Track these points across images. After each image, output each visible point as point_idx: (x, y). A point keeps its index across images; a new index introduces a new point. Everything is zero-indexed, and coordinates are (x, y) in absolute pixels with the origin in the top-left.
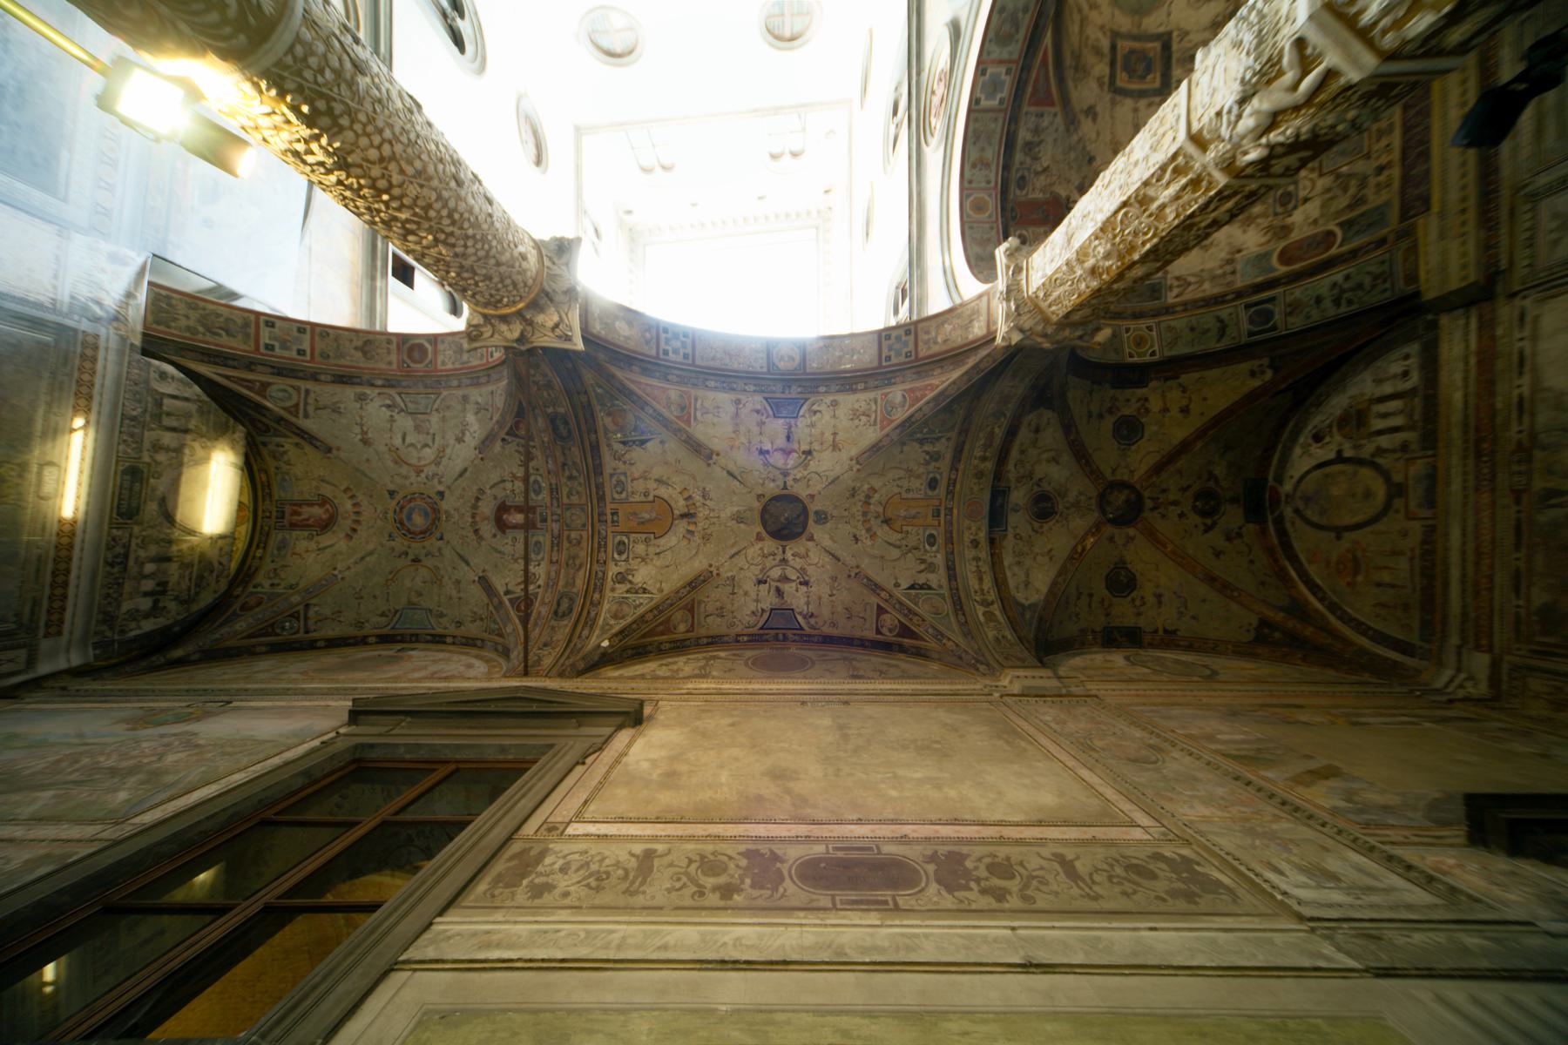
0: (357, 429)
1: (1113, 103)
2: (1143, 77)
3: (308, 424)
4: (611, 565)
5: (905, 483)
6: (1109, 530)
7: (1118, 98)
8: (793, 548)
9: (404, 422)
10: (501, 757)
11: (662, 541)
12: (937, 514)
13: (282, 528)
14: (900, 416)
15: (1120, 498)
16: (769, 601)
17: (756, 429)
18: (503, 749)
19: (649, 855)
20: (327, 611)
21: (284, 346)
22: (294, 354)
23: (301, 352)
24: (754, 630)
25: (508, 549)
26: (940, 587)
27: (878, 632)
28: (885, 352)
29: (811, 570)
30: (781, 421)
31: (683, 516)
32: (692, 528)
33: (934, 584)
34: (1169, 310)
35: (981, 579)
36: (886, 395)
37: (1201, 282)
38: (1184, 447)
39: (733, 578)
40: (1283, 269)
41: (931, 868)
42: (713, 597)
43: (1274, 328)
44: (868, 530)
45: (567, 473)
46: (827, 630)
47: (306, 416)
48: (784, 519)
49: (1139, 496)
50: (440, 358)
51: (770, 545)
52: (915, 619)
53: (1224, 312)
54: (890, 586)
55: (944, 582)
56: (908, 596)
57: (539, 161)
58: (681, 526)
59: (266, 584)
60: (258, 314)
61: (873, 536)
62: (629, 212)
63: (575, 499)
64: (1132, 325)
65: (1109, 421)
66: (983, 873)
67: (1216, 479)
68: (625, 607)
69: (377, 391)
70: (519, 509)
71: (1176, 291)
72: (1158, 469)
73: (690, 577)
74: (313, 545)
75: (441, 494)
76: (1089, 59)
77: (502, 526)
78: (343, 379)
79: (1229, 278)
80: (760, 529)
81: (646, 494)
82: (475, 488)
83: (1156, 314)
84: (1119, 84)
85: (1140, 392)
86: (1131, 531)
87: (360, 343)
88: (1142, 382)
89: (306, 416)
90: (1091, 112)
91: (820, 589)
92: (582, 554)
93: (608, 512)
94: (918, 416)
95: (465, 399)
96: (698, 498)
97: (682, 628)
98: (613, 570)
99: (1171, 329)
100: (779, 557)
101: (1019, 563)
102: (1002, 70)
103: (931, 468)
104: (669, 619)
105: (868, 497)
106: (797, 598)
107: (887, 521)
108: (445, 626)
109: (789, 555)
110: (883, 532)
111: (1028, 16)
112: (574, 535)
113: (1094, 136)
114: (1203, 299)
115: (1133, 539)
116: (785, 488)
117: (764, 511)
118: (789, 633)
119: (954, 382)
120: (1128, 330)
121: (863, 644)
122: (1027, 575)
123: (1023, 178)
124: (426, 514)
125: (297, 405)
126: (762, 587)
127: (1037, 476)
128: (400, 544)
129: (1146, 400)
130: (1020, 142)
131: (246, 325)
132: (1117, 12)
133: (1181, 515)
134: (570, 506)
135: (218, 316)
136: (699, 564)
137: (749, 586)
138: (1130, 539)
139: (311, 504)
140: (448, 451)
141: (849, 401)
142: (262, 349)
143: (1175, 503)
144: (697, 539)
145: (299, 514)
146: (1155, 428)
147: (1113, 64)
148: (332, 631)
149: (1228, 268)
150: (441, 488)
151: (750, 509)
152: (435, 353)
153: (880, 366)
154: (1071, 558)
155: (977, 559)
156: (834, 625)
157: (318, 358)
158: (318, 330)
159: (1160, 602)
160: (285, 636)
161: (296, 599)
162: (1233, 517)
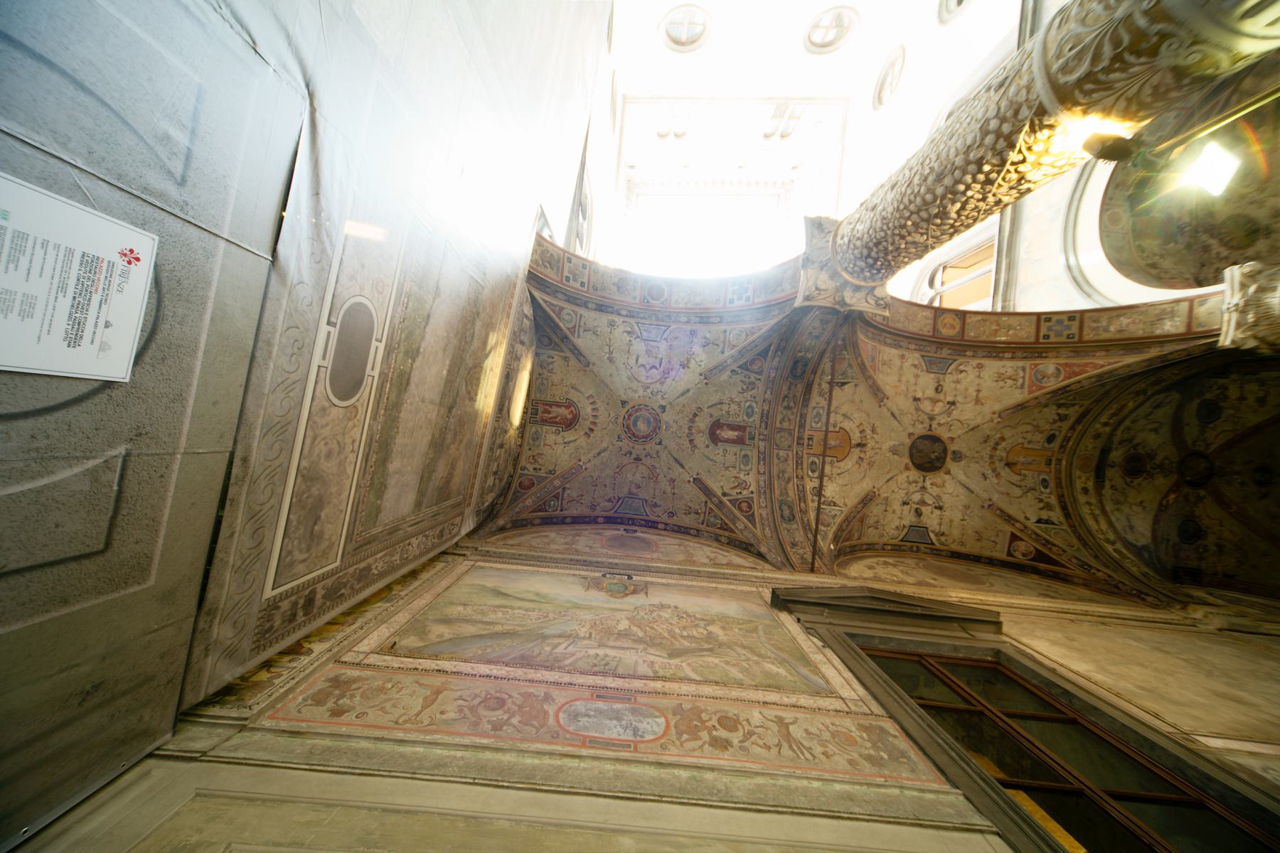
0: (606, 349)
3: (579, 342)
4: (807, 480)
5: (1029, 436)
8: (931, 478)
10: (954, 655)
11: (842, 464)
12: (1049, 463)
13: (536, 422)
14: (1052, 384)
16: (909, 519)
17: (912, 380)
18: (956, 648)
20: (574, 494)
22: (578, 285)
23: (582, 284)
25: (719, 458)
27: (1009, 554)
28: (1043, 331)
29: (945, 498)
30: (932, 375)
31: (859, 445)
33: (1055, 520)
35: (1097, 521)
36: (1036, 365)
39: (886, 499)
44: (994, 470)
45: (785, 404)
46: (955, 547)
51: (914, 474)
52: (1055, 549)
54: (1022, 518)
58: (856, 452)
59: (531, 468)
61: (998, 476)
62: (632, 167)
63: (786, 425)
70: (732, 427)
72: (1229, 445)
73: (863, 494)
74: (559, 439)
75: (663, 408)
77: (714, 439)
78: (601, 308)
80: (907, 460)
82: (694, 406)
85: (1221, 381)
86: (1202, 493)
92: (789, 469)
93: (806, 437)
94: (1073, 387)
95: (693, 333)
100: (920, 485)
101: (1118, 510)
103: (1055, 426)
105: (997, 444)
106: (931, 519)
107: (1008, 465)
108: (659, 515)
109: (928, 484)
110: (1005, 472)
112: (782, 453)
115: (1204, 497)
116: (930, 430)
117: (912, 447)
118: (922, 546)
119: (1129, 366)
121: (991, 562)
122: (1128, 520)
124: (649, 422)
126: (907, 507)
127: (1135, 442)
128: (626, 444)
134: (781, 430)
136: (866, 486)
137: (896, 506)
138: (1200, 499)
140: (673, 373)
141: (993, 367)
142: (1041, 340)
144: (865, 464)
145: (549, 413)
146: (1232, 412)
148: (575, 511)
150: (663, 403)
153: (1037, 342)
155: (1089, 504)
157: (591, 290)
160: (550, 513)
161: (557, 483)
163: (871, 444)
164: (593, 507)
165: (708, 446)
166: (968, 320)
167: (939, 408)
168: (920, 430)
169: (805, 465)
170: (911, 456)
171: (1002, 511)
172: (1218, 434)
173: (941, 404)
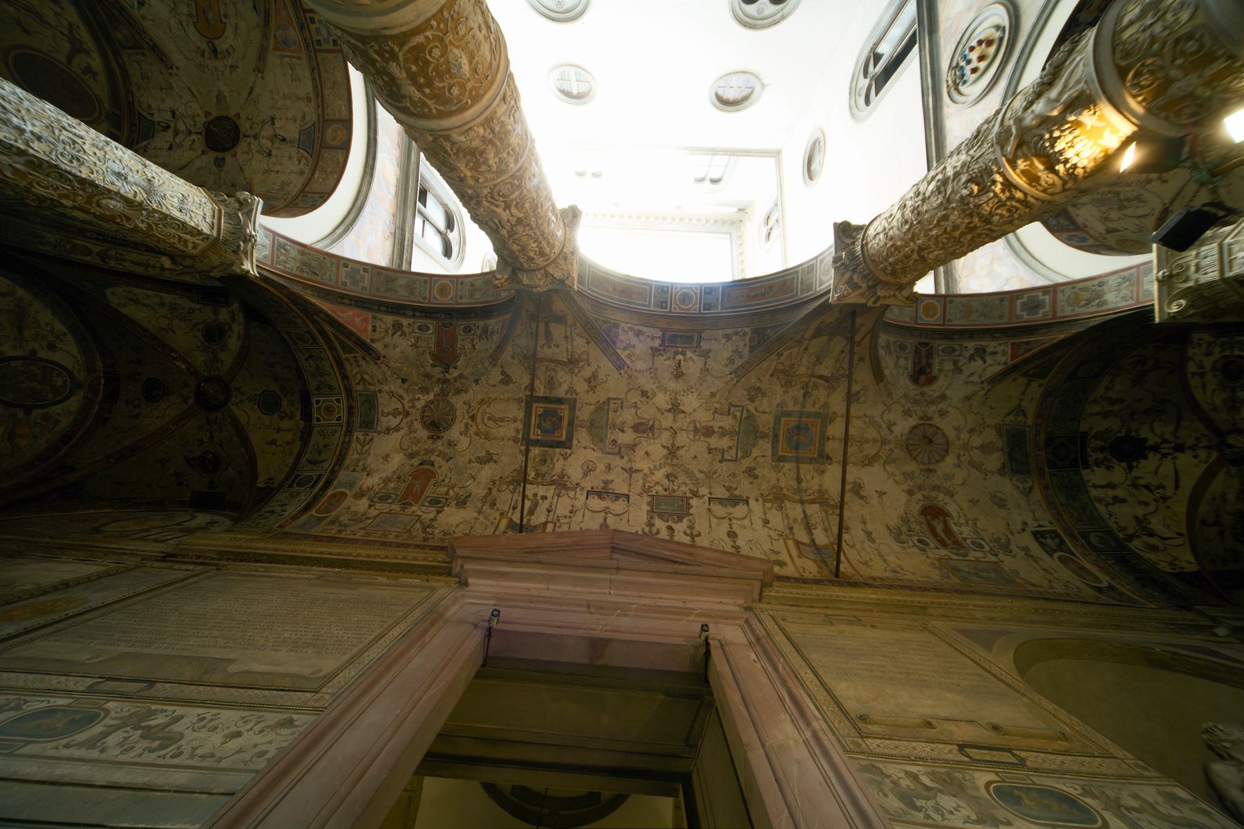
1: (519, 401)
2: (539, 427)
8: (199, 140)
11: (192, 28)
30: (297, 136)
34: (349, 432)
35: (138, 264)
38: (245, 440)
39: (172, 88)
71: (361, 437)
80: (215, 113)
84: (535, 405)
86: (191, 401)
90: (507, 380)
96: (229, 62)
99: (334, 433)
100: (192, 129)
113: (492, 382)
116: (245, 136)
117: (227, 118)
120: (338, 401)
132: (593, 407)
133: (201, 441)
136: (177, 58)
143: (212, 437)
147: (546, 399)
166: (339, 152)
167: (266, 143)
168: (244, 126)
170: (219, 118)
173: (269, 145)
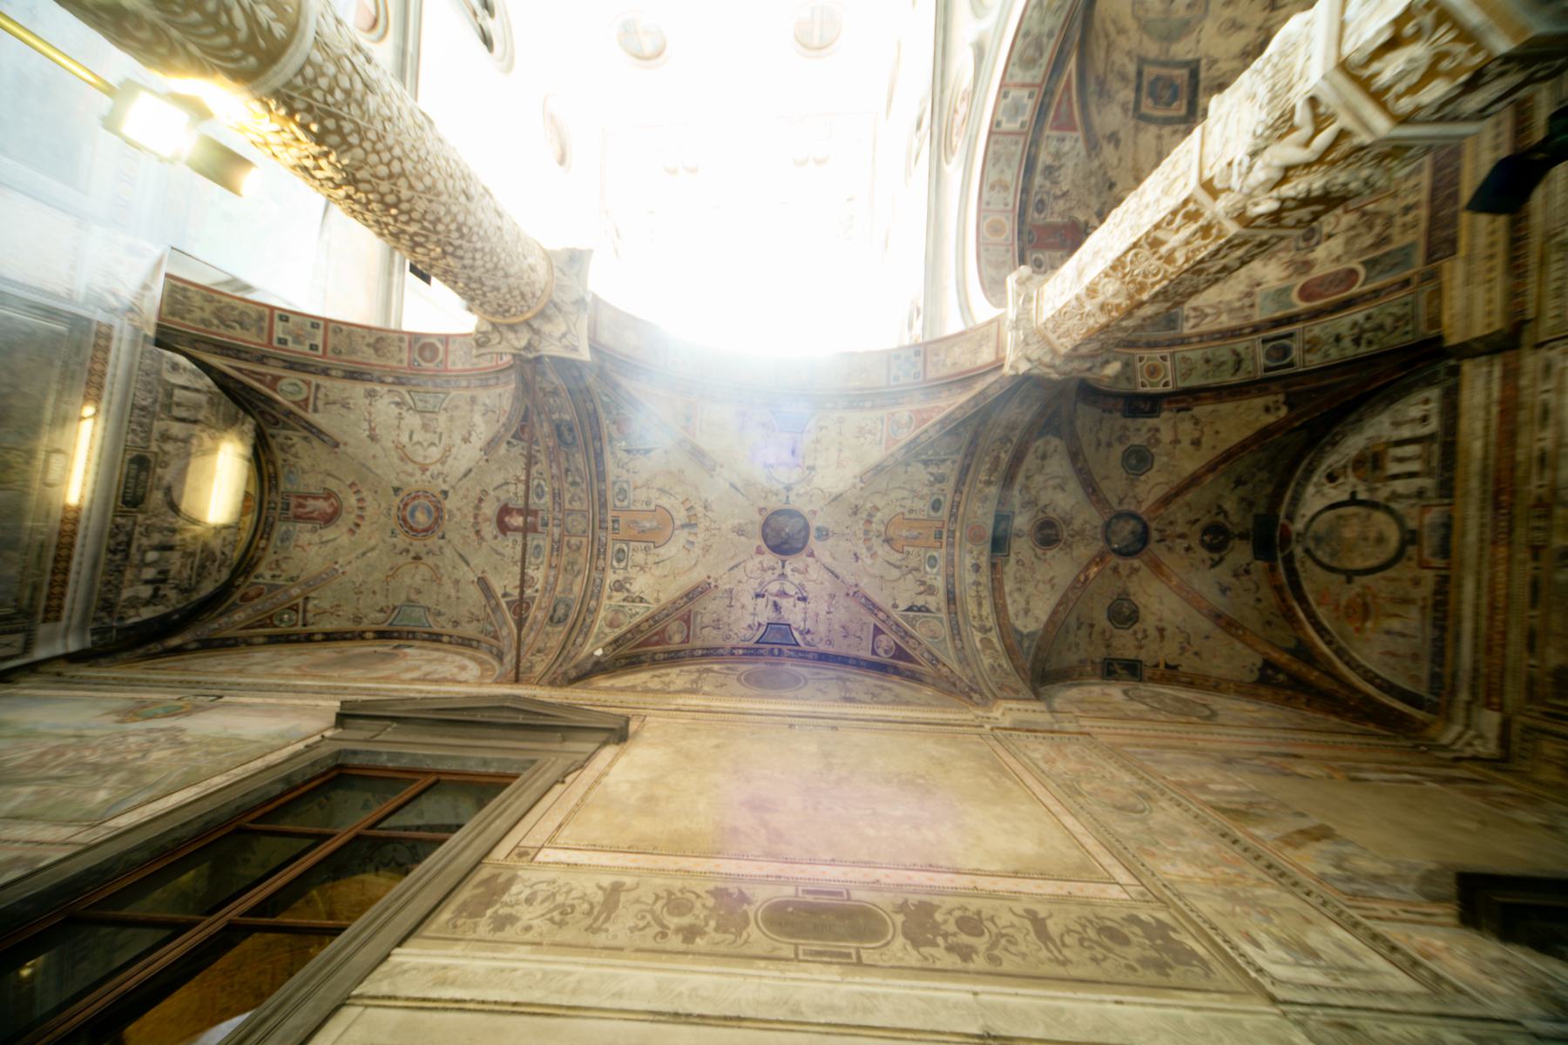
0: (365, 425)
1: (1137, 129)
2: (1169, 104)
3: (317, 419)
4: (609, 572)
5: (908, 503)
6: (1114, 560)
7: (1142, 124)
8: (793, 562)
9: (412, 420)
10: (483, 770)
11: (661, 551)
12: (939, 536)
13: (287, 519)
14: (905, 436)
15: (1126, 529)
16: (766, 615)
18: (485, 762)
19: (617, 888)
20: (326, 605)
21: (297, 340)
22: (306, 349)
23: (313, 347)
24: (750, 644)
25: (508, 551)
26: (939, 610)
27: (874, 652)
29: (809, 586)
31: (683, 526)
32: (692, 538)
34: (1184, 341)
35: (980, 605)
37: (1219, 314)
38: (1194, 480)
39: (731, 591)
40: (1302, 306)
41: (900, 919)
42: (710, 608)
43: (1291, 365)
44: (869, 549)
45: (570, 479)
46: (823, 648)
47: (316, 410)
48: (783, 537)
49: (1146, 529)
50: (451, 358)
51: (770, 559)
52: (911, 642)
53: (1241, 345)
54: (888, 606)
55: (943, 605)
56: (906, 618)
57: (562, 161)
58: (682, 536)
59: (268, 574)
60: (272, 309)
61: (874, 555)
63: (577, 505)
64: (1146, 353)
65: (1119, 450)
66: (951, 927)
67: (1226, 514)
68: (621, 617)
69: (386, 388)
70: (520, 512)
71: (1192, 322)
72: (1166, 501)
73: (690, 586)
74: (315, 538)
75: (445, 493)
76: (1114, 84)
77: (503, 528)
78: (353, 375)
79: (1247, 311)
80: (760, 542)
81: (648, 503)
82: (479, 489)
83: (1171, 344)
85: (1151, 422)
86: (1136, 563)
87: (372, 340)
88: (1153, 412)
89: (316, 410)
90: (1114, 138)
91: (818, 606)
92: (581, 560)
93: (609, 519)
94: (923, 438)
95: (473, 400)
96: (699, 509)
97: (677, 638)
98: (611, 577)
99: (1185, 360)
100: (778, 572)
101: (1019, 590)
102: (1025, 93)
104: (664, 630)
105: (870, 515)
106: (794, 614)
107: (888, 541)
108: (441, 625)
109: (788, 570)
110: (883, 550)
111: (1053, 41)
112: (574, 541)
113: (1115, 161)
114: (1219, 332)
116: (787, 502)
117: (766, 524)
119: (961, 407)
120: (1141, 359)
122: (1028, 603)
123: (1041, 201)
124: (429, 512)
125: (306, 400)
127: (1043, 501)
128: (401, 540)
129: (1157, 430)
130: (1040, 166)
131: (261, 318)
132: (1145, 38)
133: (1188, 549)
134: (572, 511)
135: (233, 308)
137: (747, 599)
138: (1135, 571)
139: (316, 497)
140: (454, 450)
143: (1182, 536)
144: (697, 551)
145: (303, 506)
146: (1165, 459)
147: (1138, 89)
148: (329, 625)
149: (1247, 302)
150: (445, 487)
151: (752, 523)
152: (446, 352)
154: (1072, 587)
156: (830, 642)
157: (330, 353)
158: (331, 325)
159: (1162, 637)
160: (284, 628)
161: (295, 591)
162: (1240, 553)
163: (703, 524)
164: (357, 619)
165: (496, 537)
169: (609, 554)
170: (765, 537)
171: (867, 599)
172: (1152, 487)
